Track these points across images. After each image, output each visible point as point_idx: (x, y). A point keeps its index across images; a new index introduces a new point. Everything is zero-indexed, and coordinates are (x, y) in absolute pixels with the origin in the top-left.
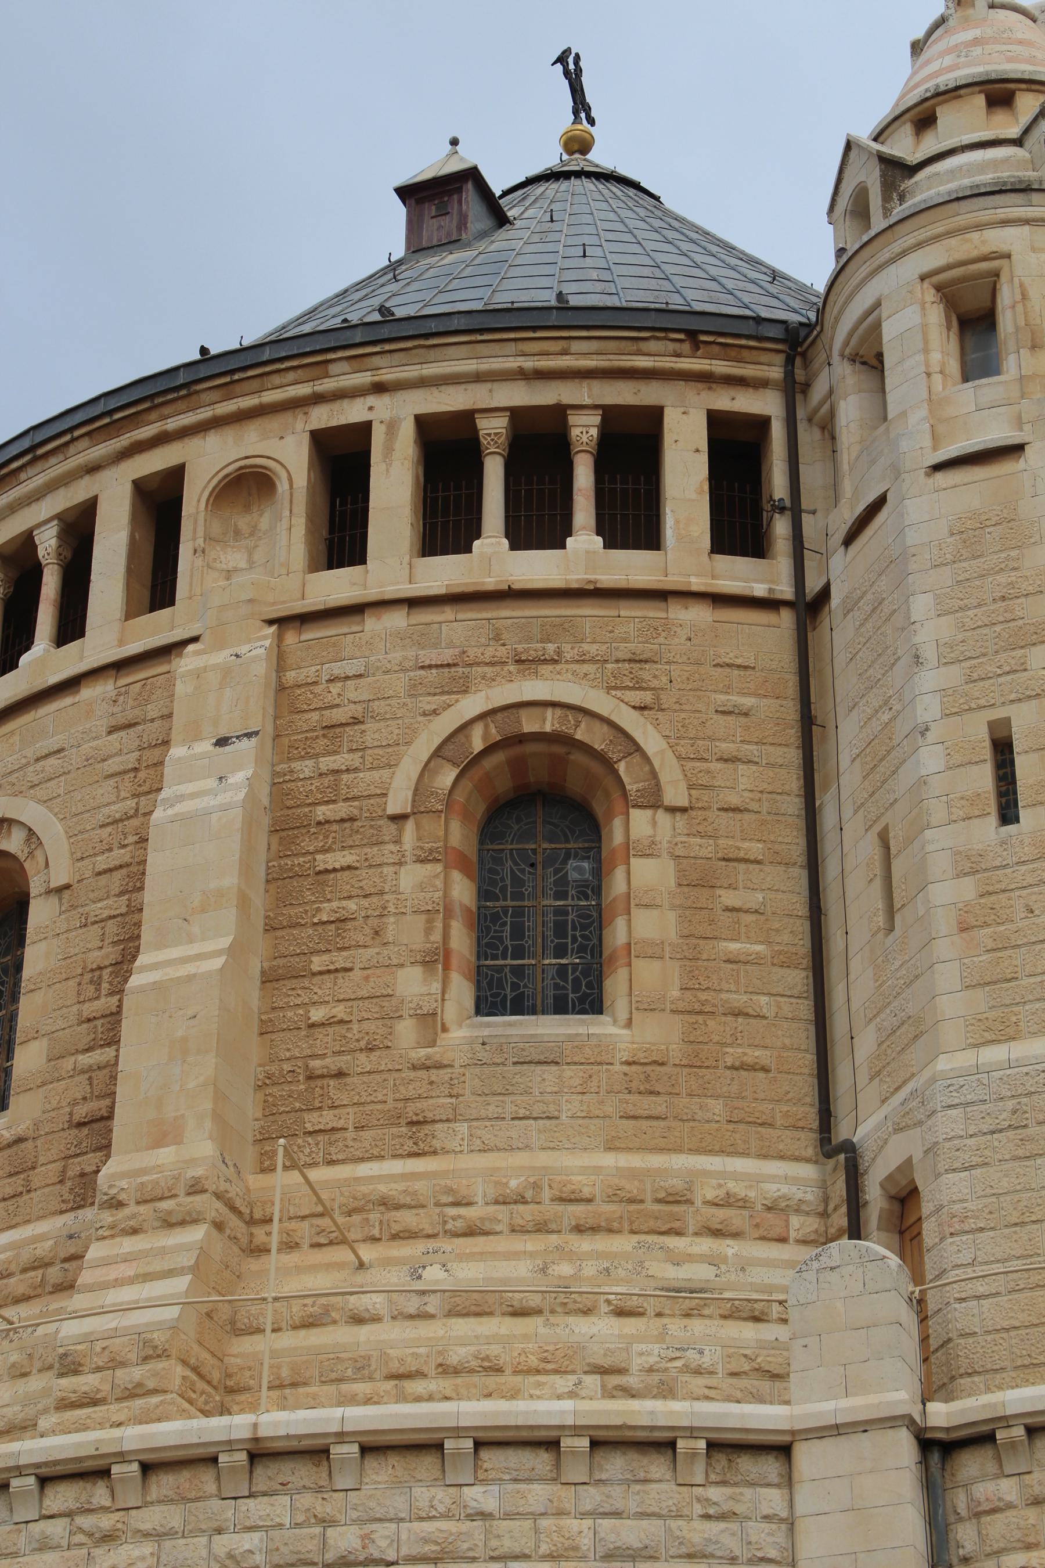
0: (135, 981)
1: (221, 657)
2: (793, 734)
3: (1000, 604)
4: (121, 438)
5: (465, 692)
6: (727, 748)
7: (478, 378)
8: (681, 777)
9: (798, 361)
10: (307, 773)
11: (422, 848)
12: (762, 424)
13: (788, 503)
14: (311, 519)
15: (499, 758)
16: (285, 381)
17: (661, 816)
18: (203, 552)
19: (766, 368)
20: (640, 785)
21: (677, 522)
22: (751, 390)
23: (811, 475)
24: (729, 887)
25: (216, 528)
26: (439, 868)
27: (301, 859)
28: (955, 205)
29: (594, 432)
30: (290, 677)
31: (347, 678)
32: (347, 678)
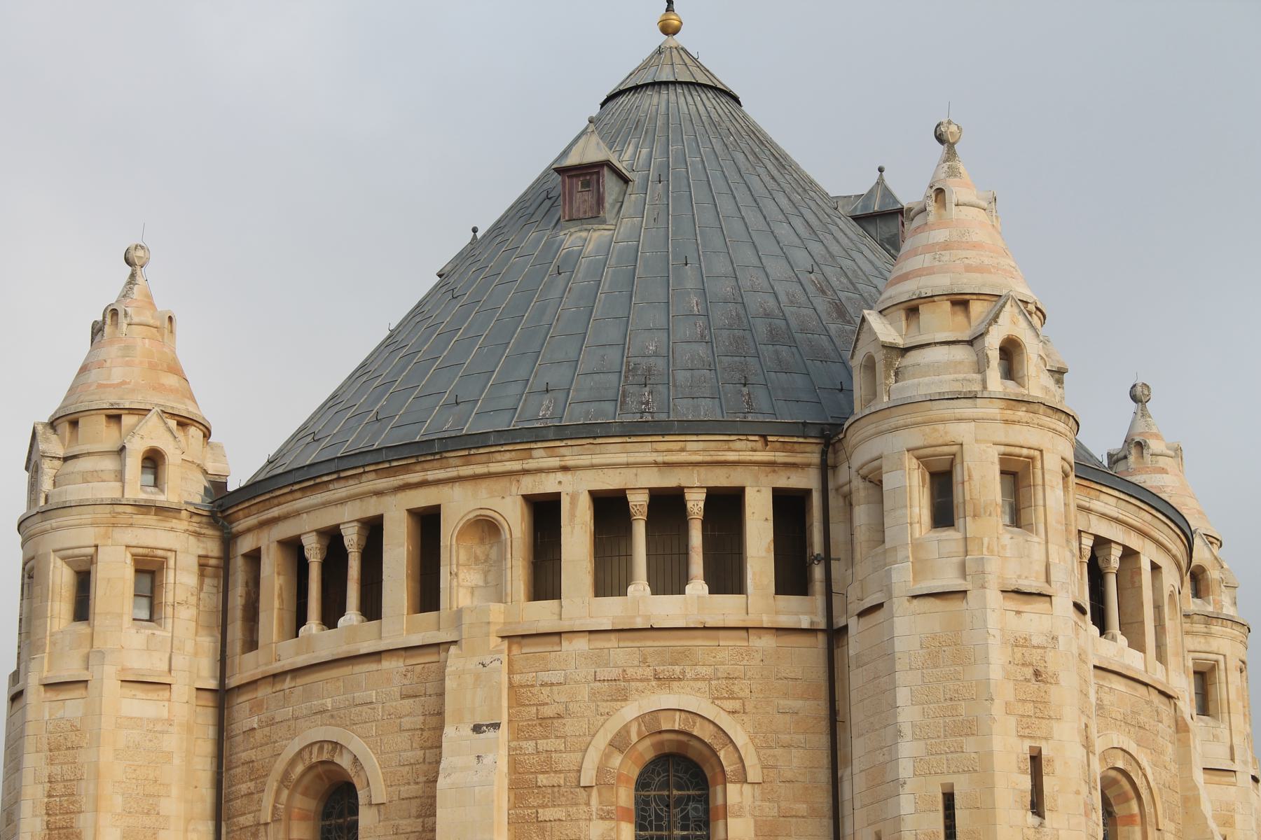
1: (472, 664)
2: (824, 725)
3: (949, 703)
4: (397, 478)
5: (626, 700)
6: (785, 738)
7: (628, 465)
8: (757, 762)
9: (830, 449)
10: (530, 751)
11: (602, 810)
12: (808, 492)
15: (648, 742)
16: (504, 458)
17: (745, 786)
18: (456, 575)
19: (809, 455)
20: (732, 768)
21: (754, 574)
22: (800, 470)
24: (787, 835)
25: (463, 556)
26: (613, 824)
27: (530, 811)
28: (929, 403)
29: (702, 504)
32: (552, 684)
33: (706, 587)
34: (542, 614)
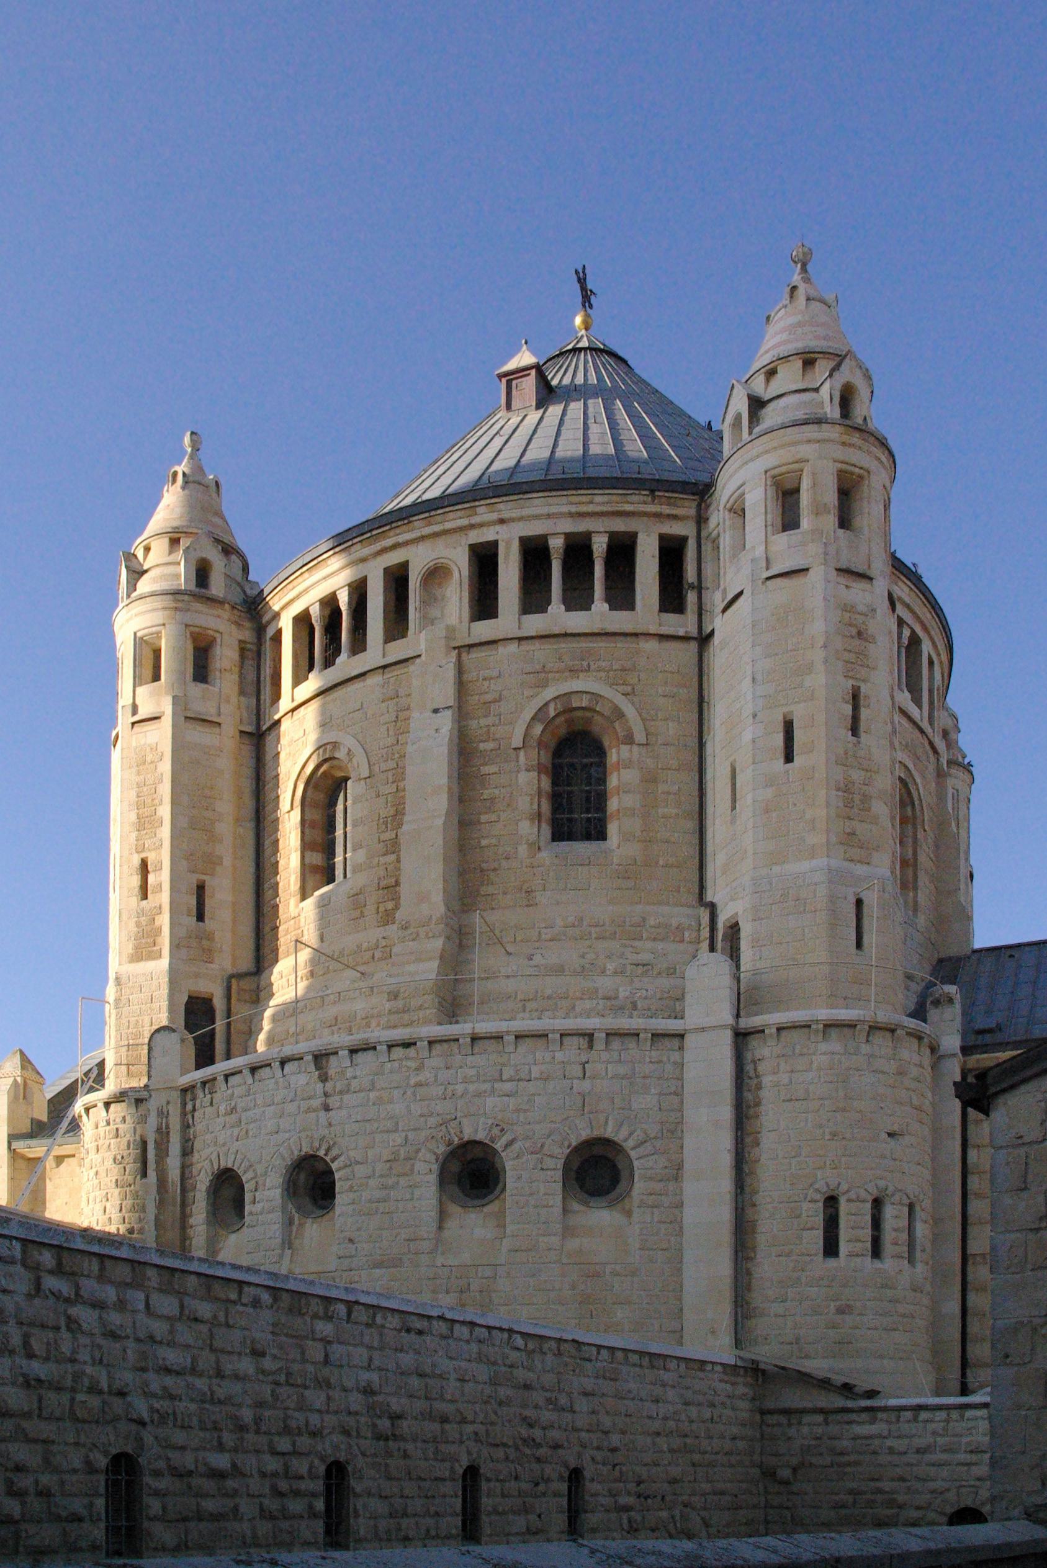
0: (405, 827)
13: (696, 584)
14: (471, 593)
15: (562, 718)
21: (643, 598)
23: (708, 570)
30: (465, 677)
31: (491, 678)
32: (491, 678)
33: (606, 606)
34: (484, 629)
